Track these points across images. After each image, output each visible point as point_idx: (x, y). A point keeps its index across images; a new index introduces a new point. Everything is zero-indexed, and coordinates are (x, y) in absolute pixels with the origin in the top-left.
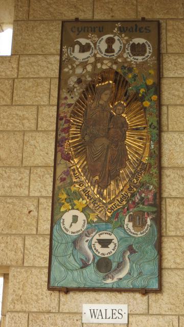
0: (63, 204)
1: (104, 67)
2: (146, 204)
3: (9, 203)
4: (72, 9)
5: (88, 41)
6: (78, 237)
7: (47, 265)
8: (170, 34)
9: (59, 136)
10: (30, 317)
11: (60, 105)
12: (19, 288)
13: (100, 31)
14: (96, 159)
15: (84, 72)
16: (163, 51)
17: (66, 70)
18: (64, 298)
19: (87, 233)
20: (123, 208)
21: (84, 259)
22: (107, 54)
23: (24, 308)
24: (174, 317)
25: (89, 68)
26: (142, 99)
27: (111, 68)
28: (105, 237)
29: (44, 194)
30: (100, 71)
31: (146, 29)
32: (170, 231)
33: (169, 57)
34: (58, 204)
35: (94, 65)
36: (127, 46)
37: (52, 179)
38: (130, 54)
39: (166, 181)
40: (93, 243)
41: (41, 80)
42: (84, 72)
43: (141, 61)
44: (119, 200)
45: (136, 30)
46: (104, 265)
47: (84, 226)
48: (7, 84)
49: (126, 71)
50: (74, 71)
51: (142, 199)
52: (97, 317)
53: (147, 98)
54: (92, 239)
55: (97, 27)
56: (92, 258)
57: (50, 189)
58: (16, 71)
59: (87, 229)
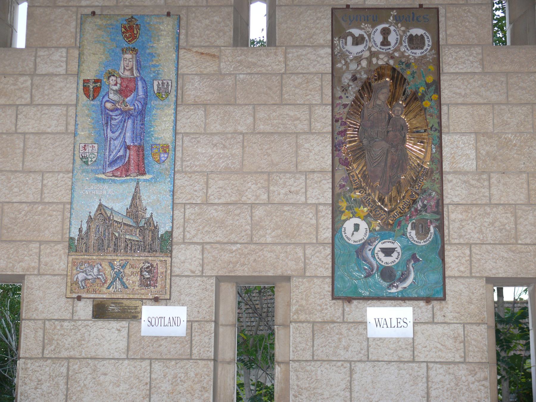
0: (343, 212)
1: (380, 63)
2: (429, 211)
3: (286, 211)
5: (362, 32)
7: (331, 275)
11: (335, 105)
12: (302, 299)
14: (375, 164)
15: (359, 68)
17: (339, 65)
22: (382, 47)
23: (308, 318)
24: (459, 325)
26: (422, 99)
29: (321, 201)
30: (376, 68)
32: (453, 239)
33: (449, 49)
34: (338, 212)
36: (404, 38)
38: (408, 47)
39: (447, 187)
40: (376, 251)
43: (420, 55)
44: (401, 207)
45: (413, 19)
46: (388, 274)
47: (366, 234)
49: (404, 66)
50: (348, 67)
51: (424, 206)
52: (382, 326)
53: (427, 97)
56: (376, 266)
59: (369, 237)
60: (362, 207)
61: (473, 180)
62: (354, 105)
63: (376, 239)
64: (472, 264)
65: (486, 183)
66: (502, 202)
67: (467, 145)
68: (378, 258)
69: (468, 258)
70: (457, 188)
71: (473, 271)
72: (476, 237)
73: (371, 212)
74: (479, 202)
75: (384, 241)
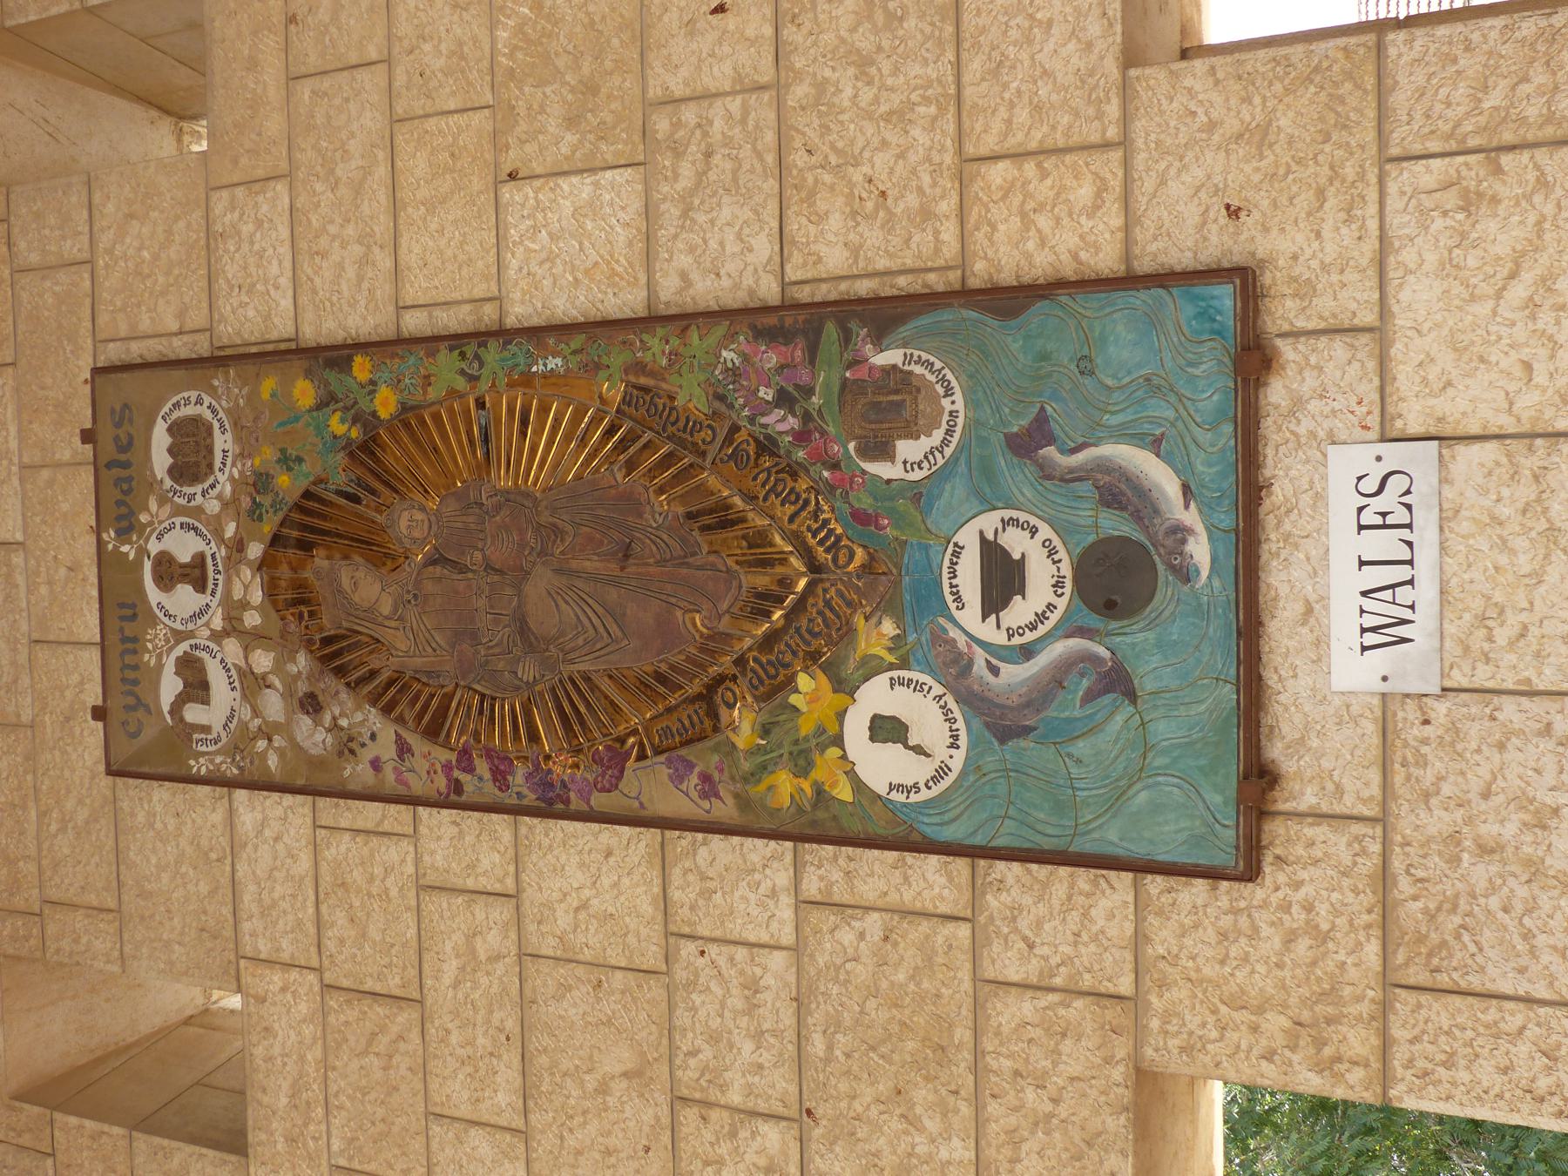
0: (819, 791)
1: (257, 596)
2: (804, 376)
3: (830, 1048)
6: (978, 712)
7: (1127, 877)
9: (525, 802)
10: (1412, 981)
11: (401, 790)
12: (1255, 1029)
14: (613, 629)
15: (277, 683)
16: (203, 348)
17: (273, 761)
18: (1300, 793)
19: (954, 670)
21: (1085, 683)
22: (210, 586)
23: (1364, 1008)
24: (1392, 188)
25: (263, 661)
26: (368, 421)
29: (783, 878)
30: (274, 615)
31: (118, 425)
32: (937, 251)
33: (223, 319)
34: (821, 815)
35: (252, 639)
36: (181, 501)
37: (716, 841)
38: (206, 485)
39: (708, 291)
40: (1000, 638)
41: (324, 867)
42: (277, 683)
43: (229, 436)
44: (790, 509)
45: (126, 465)
46: (1115, 580)
47: (919, 687)
48: (342, 1018)
49: (266, 501)
50: (277, 727)
51: (784, 399)
52: (1406, 614)
53: (364, 404)
55: (122, 630)
57: (758, 849)
58: (294, 974)
59: (931, 672)
60: (794, 699)
61: (676, 176)
62: (398, 710)
63: (939, 638)
64: (1061, 144)
65: (689, 114)
66: (768, 31)
67: (540, 216)
68: (1033, 627)
69: (1030, 168)
70: (713, 244)
71: (1095, 138)
72: (927, 139)
73: (814, 656)
74: (770, 137)
75: (949, 599)
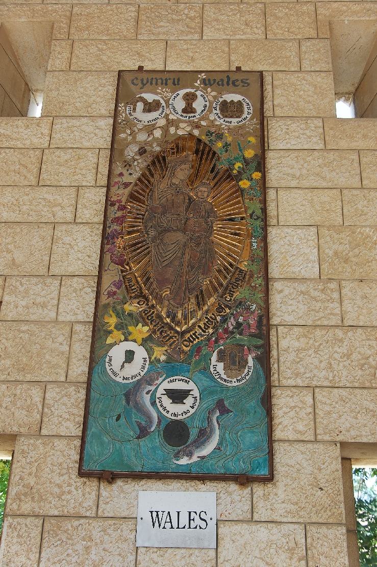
1: (180, 133)
2: (246, 332)
3: (23, 332)
4: (135, 58)
5: (157, 98)
6: (135, 387)
8: (278, 91)
9: (107, 229)
10: (45, 525)
12: (30, 474)
13: (174, 84)
14: (166, 263)
15: (150, 139)
16: (268, 113)
17: (123, 136)
18: (107, 491)
19: (148, 380)
20: (209, 340)
21: (143, 423)
22: (184, 115)
23: (37, 510)
24: (296, 526)
25: (158, 133)
26: (238, 178)
27: (191, 135)
28: (179, 385)
31: (242, 81)
32: (285, 378)
34: (102, 333)
35: (165, 129)
36: (214, 105)
37: (94, 295)
38: (219, 115)
39: (276, 300)
40: (158, 395)
41: (85, 151)
42: (150, 139)
43: (236, 124)
45: (228, 84)
46: (176, 433)
48: (32, 156)
50: (134, 138)
51: (239, 325)
52: (162, 526)
53: (244, 176)
54: (157, 388)
55: (170, 79)
56: (156, 420)
57: (91, 309)
58: (48, 138)
60: (140, 325)
61: (315, 290)
62: (139, 184)
63: (159, 375)
64: (317, 420)
65: (336, 295)
66: (361, 324)
67: (305, 241)
68: (161, 406)
69: (310, 410)
70: (291, 302)
71: (318, 432)
72: (322, 377)
73: (154, 332)
74: (326, 323)
75: (172, 378)
